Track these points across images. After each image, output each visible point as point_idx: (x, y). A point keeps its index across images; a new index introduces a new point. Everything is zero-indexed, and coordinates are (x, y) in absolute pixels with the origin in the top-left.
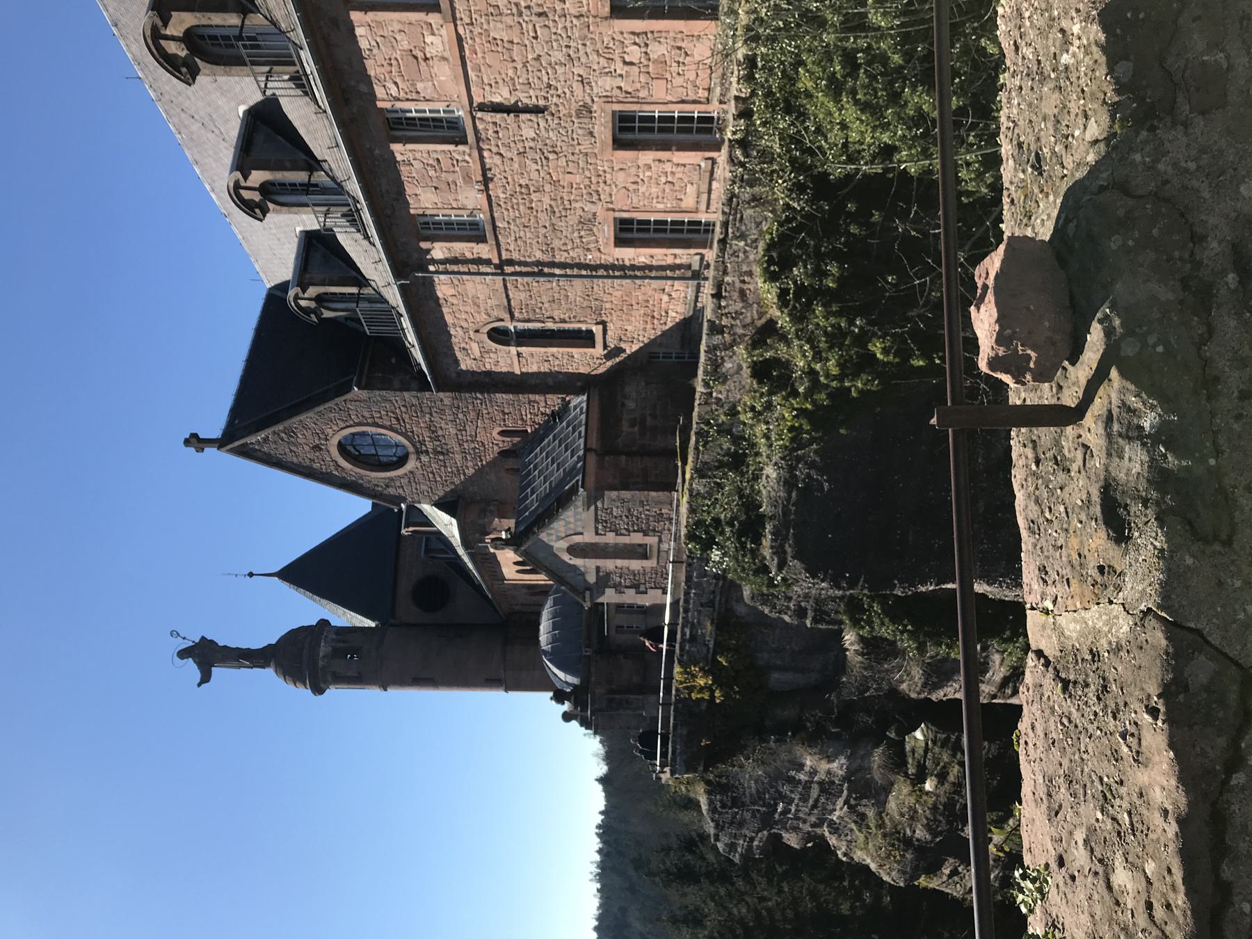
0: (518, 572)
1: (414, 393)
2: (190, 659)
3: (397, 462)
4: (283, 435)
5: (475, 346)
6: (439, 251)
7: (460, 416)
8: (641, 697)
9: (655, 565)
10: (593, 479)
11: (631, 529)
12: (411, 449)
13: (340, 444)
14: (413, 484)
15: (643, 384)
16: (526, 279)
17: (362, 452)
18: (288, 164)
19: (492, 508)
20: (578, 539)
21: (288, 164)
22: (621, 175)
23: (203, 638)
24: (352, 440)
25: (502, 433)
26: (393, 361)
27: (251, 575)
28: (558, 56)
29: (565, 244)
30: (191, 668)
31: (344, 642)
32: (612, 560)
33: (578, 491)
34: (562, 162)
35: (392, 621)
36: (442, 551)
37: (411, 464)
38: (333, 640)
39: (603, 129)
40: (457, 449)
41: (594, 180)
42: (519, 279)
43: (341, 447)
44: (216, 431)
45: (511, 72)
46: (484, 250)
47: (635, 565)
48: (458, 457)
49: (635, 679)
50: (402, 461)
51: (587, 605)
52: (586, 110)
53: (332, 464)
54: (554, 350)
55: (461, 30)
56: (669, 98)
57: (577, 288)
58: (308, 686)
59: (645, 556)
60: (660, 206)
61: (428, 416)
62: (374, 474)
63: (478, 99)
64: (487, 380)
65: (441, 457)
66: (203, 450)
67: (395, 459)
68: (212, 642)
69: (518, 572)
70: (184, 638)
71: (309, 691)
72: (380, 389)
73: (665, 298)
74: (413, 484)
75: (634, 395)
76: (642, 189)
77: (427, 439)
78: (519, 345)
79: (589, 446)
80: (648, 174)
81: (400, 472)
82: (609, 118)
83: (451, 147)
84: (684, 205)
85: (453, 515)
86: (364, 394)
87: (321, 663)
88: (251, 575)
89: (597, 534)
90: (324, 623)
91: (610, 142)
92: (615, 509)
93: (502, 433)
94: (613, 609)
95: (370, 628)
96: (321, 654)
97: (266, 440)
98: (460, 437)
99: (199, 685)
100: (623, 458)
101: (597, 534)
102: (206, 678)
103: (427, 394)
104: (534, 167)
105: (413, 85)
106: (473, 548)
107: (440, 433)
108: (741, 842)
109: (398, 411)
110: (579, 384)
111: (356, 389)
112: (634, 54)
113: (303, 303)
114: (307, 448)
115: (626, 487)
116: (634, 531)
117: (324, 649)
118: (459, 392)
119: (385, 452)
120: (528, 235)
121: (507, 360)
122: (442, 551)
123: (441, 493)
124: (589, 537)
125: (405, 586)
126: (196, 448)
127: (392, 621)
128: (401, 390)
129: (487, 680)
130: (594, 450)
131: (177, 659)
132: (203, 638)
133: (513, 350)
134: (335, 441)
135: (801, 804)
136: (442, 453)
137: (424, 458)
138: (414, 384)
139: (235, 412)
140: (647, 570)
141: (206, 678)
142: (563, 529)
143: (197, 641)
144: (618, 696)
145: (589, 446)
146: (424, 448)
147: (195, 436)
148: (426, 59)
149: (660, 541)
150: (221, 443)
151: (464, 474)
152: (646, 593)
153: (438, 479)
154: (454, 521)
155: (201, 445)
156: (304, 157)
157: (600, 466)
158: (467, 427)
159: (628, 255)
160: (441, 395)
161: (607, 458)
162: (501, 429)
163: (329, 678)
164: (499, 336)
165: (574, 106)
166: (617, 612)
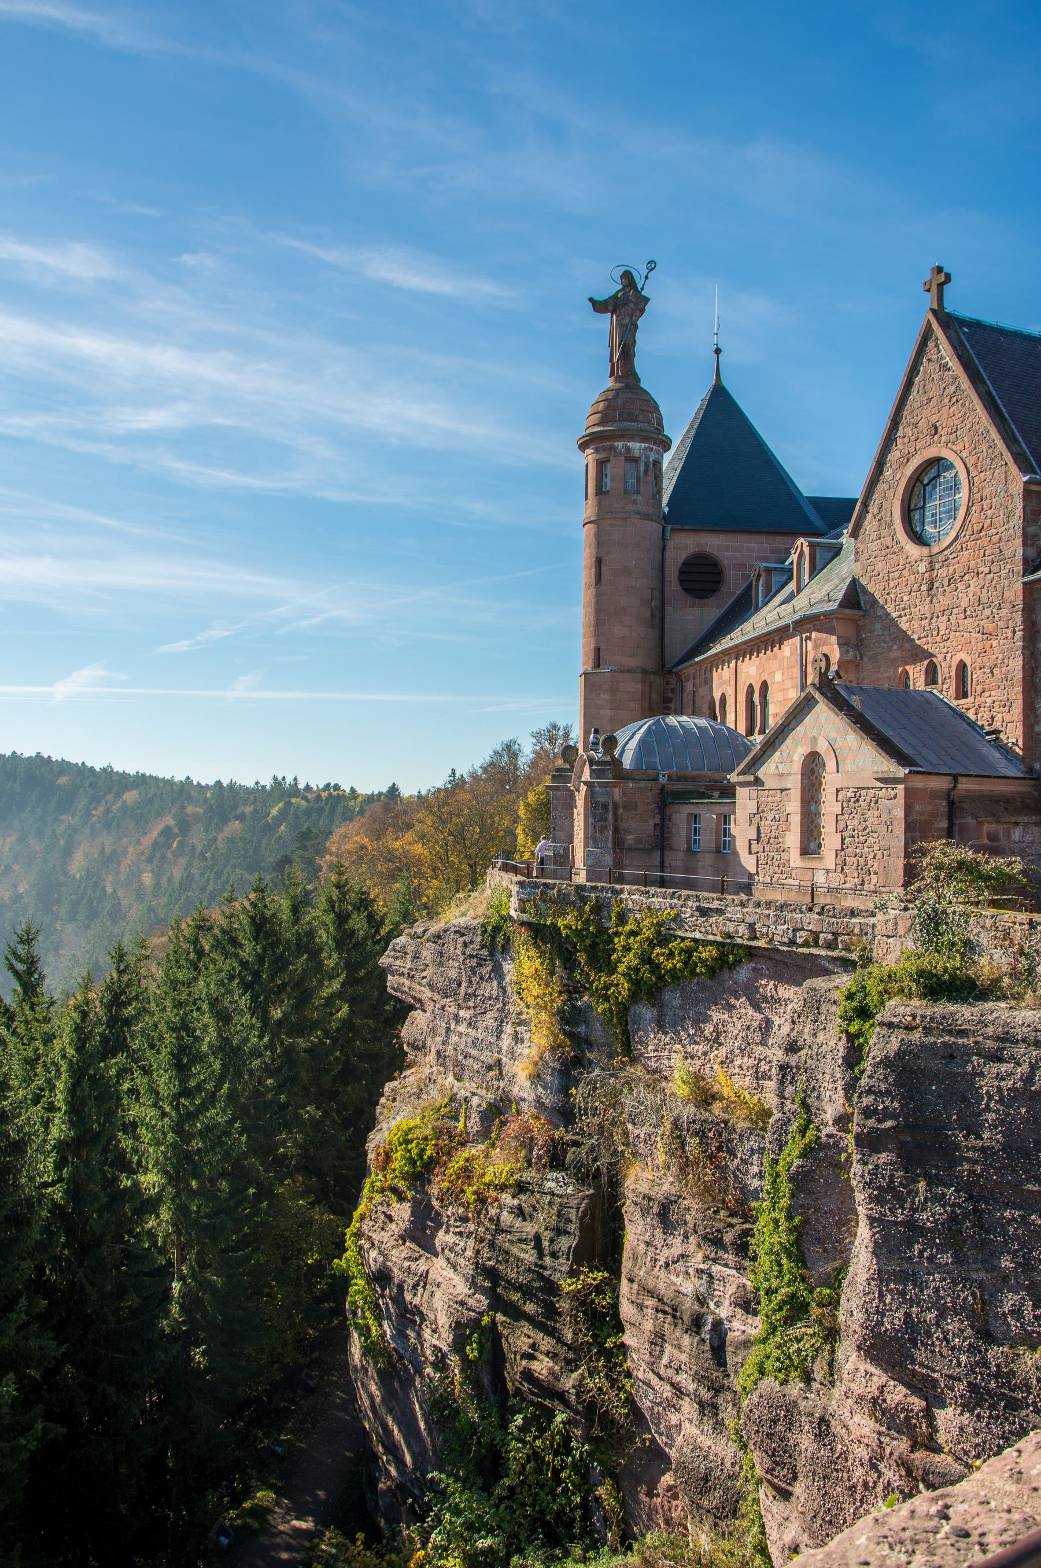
0: (751, 686)
2: (621, 287)
3: (915, 533)
4: (953, 389)
7: (987, 612)
8: (610, 845)
9: (792, 864)
11: (846, 834)
12: (935, 549)
14: (884, 553)
17: (928, 489)
19: (851, 653)
20: (830, 765)
23: (647, 300)
25: (965, 666)
27: (718, 351)
30: (610, 288)
31: (646, 471)
32: (799, 809)
33: (903, 765)
35: (669, 528)
37: (913, 550)
38: (647, 457)
40: (938, 608)
44: (949, 308)
47: (793, 839)
48: (925, 608)
49: (630, 838)
50: (919, 539)
51: (733, 777)
53: (912, 450)
58: (588, 431)
59: (805, 852)
61: (987, 570)
62: (897, 504)
65: (924, 587)
66: (928, 290)
68: (642, 311)
69: (751, 686)
70: (646, 278)
71: (584, 433)
72: (1024, 508)
74: (884, 553)
75: (1029, 838)
79: (960, 778)
81: (902, 536)
85: (842, 605)
87: (619, 444)
88: (718, 351)
90: (666, 444)
92: (876, 813)
93: (962, 667)
94: (725, 809)
95: (660, 501)
96: (631, 444)
97: (945, 367)
98: (955, 611)
99: (591, 300)
100: (944, 824)
101: (838, 791)
102: (599, 306)
103: (1019, 568)
106: (794, 629)
107: (961, 586)
108: (409, 965)
109: (993, 531)
111: (1025, 479)
114: (934, 419)
115: (909, 827)
116: (843, 840)
117: (637, 447)
118: (1023, 610)
123: (870, 588)
124: (831, 779)
126: (931, 282)
127: (669, 528)
128: (1025, 535)
129: (599, 649)
130: (955, 786)
131: (622, 270)
132: (647, 300)
135: (470, 1040)
137: (922, 567)
138: (1032, 552)
139: (977, 327)
140: (784, 855)
141: (599, 306)
143: (643, 293)
144: (610, 816)
145: (960, 778)
146: (937, 566)
147: (948, 278)
149: (828, 871)
150: (939, 313)
151: (900, 616)
152: (750, 853)
153: (892, 584)
154: (833, 606)
155: (934, 289)
157: (934, 795)
158: (971, 620)
160: (1019, 586)
161: (944, 803)
163: (602, 456)
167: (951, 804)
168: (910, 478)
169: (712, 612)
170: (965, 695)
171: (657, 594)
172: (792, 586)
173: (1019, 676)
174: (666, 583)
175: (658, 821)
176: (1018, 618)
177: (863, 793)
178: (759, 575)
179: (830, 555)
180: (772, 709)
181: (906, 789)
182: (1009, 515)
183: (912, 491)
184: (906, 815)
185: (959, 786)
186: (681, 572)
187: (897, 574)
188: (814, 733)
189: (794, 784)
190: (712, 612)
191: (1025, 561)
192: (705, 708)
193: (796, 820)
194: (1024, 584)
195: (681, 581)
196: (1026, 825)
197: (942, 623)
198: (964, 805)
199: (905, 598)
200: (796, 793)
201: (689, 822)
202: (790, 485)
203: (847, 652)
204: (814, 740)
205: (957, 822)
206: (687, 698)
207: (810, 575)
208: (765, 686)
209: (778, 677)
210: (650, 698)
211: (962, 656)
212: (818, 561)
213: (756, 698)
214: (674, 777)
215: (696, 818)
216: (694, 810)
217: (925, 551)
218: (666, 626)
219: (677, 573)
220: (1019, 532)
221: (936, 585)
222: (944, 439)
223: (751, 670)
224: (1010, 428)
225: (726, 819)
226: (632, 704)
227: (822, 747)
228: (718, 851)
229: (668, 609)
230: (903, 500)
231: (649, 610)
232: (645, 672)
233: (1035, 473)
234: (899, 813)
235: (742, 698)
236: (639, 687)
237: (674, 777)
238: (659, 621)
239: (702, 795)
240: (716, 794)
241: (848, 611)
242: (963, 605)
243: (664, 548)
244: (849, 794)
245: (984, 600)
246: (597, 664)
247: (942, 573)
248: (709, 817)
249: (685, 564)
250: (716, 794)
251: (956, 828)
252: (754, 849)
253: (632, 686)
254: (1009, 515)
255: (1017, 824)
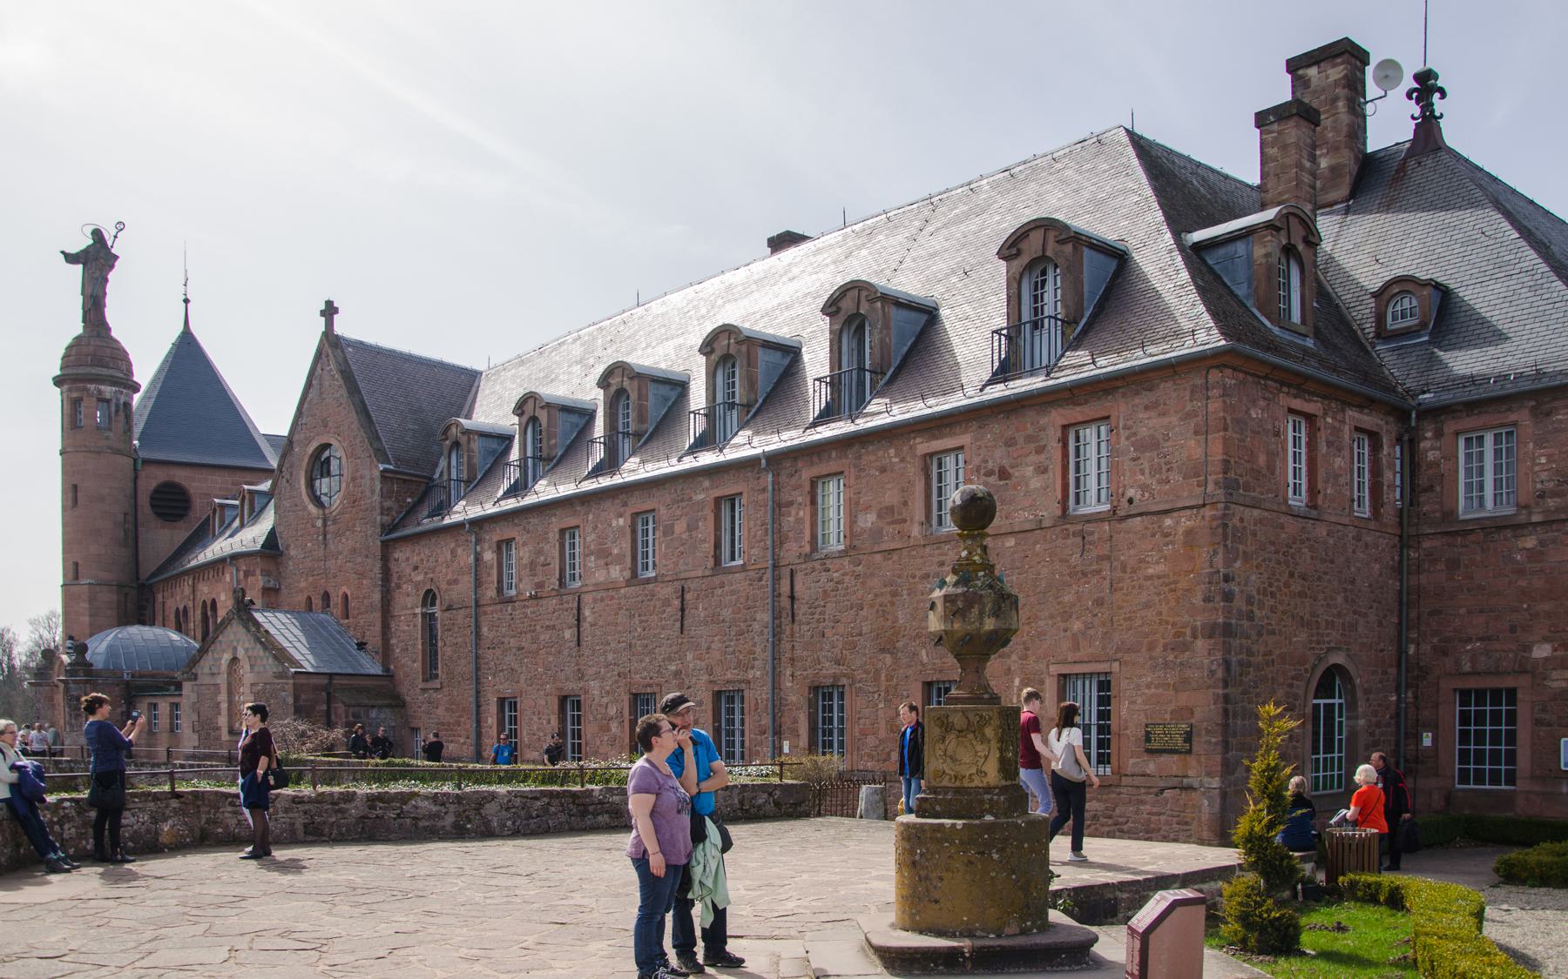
1: (379, 518)
5: (420, 578)
6: (489, 556)
7: (359, 560)
10: (304, 681)
13: (330, 445)
15: (393, 724)
16: (473, 625)
18: (553, 442)
21: (553, 442)
22: (542, 702)
24: (335, 457)
25: (347, 596)
26: (409, 500)
28: (610, 657)
29: (498, 659)
32: (226, 699)
34: (551, 659)
36: (222, 521)
37: (312, 508)
39: (571, 686)
41: (540, 682)
42: (473, 620)
43: (327, 446)
45: (601, 623)
46: (490, 593)
47: (223, 721)
50: (317, 501)
52: (581, 676)
54: (420, 647)
55: (622, 591)
56: (589, 736)
57: (465, 666)
60: (525, 733)
62: (303, 473)
63: (587, 598)
64: (393, 585)
65: (321, 538)
67: (318, 493)
72: (381, 489)
73: (462, 740)
74: (294, 509)
76: (535, 718)
77: (338, 526)
78: (424, 615)
80: (545, 722)
82: (577, 693)
83: (557, 576)
84: (525, 750)
85: (263, 546)
86: (377, 474)
89: (252, 685)
91: (564, 694)
93: (346, 596)
94: (176, 700)
98: (340, 557)
100: (324, 707)
101: (252, 685)
104: (548, 637)
105: (592, 554)
110: (392, 667)
111: (381, 467)
112: (612, 711)
113: (454, 429)
119: (324, 486)
120: (504, 629)
121: (408, 605)
122: (222, 521)
125: (180, 476)
128: (382, 508)
130: (330, 683)
133: (418, 610)
134: (333, 441)
136: (325, 539)
137: (319, 523)
142: (255, 654)
146: (329, 523)
148: (607, 564)
154: (258, 547)
156: (559, 454)
157: (316, 688)
159: (491, 710)
160: (379, 543)
161: (324, 693)
162: (349, 594)
164: (430, 597)
165: (582, 667)
166: (172, 704)
167: (329, 694)
168: (311, 456)
169: (180, 534)
170: (348, 618)
171: (130, 518)
172: (237, 523)
173: (379, 605)
174: (139, 508)
175: (124, 709)
176: (378, 564)
177: (268, 687)
178: (215, 511)
179: (265, 501)
180: (219, 620)
181: (294, 684)
182: (373, 492)
183: (313, 466)
184: (295, 702)
185: (335, 682)
186: (152, 498)
187: (303, 526)
188: (235, 643)
189: (222, 680)
190: (180, 534)
191: (382, 526)
192: (172, 617)
193: (224, 706)
194: (382, 542)
195: (153, 506)
196: (380, 707)
197: (331, 564)
198: (337, 695)
199: (309, 545)
200: (224, 688)
201: (149, 710)
202: (250, 426)
203: (269, 581)
204: (235, 649)
205: (333, 705)
206: (158, 607)
207: (250, 515)
208: (214, 602)
209: (223, 597)
210: (126, 606)
211: (344, 589)
212: (256, 505)
213: (209, 613)
214: (137, 675)
215: (155, 706)
216: (154, 700)
217: (321, 512)
218: (140, 545)
219: (148, 499)
220: (378, 506)
221: (328, 536)
222: (332, 431)
223: (205, 591)
224: (375, 428)
225: (176, 706)
226: (109, 612)
227: (241, 653)
228: (172, 731)
229: (141, 529)
230: (306, 472)
231: (123, 533)
232: (120, 586)
233: (390, 464)
234: (290, 700)
235: (199, 612)
236: (115, 597)
237: (137, 675)
238: (132, 538)
239: (160, 689)
240: (172, 688)
241: (268, 551)
242: (345, 553)
243: (136, 478)
244: (259, 688)
245: (357, 551)
246: (76, 577)
247: (331, 528)
248: (164, 706)
249: (156, 491)
250: (172, 688)
251: (332, 710)
252: (196, 729)
253: (108, 597)
254: (373, 492)
255: (373, 707)
